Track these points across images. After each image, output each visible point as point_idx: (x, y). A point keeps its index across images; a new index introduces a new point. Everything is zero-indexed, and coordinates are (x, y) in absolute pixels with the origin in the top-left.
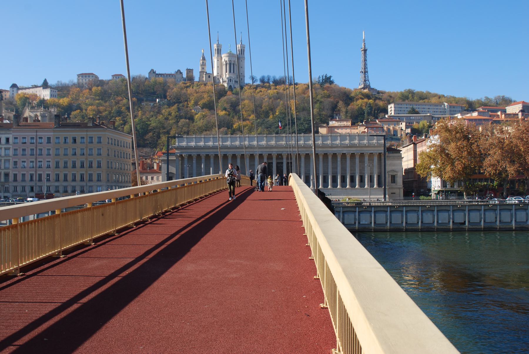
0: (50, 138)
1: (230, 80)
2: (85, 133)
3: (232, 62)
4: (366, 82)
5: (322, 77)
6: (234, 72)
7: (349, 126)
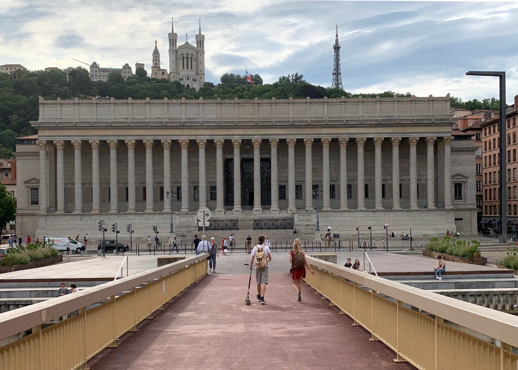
1: (188, 77)
3: (190, 56)
4: (339, 86)
5: (292, 77)
6: (191, 69)
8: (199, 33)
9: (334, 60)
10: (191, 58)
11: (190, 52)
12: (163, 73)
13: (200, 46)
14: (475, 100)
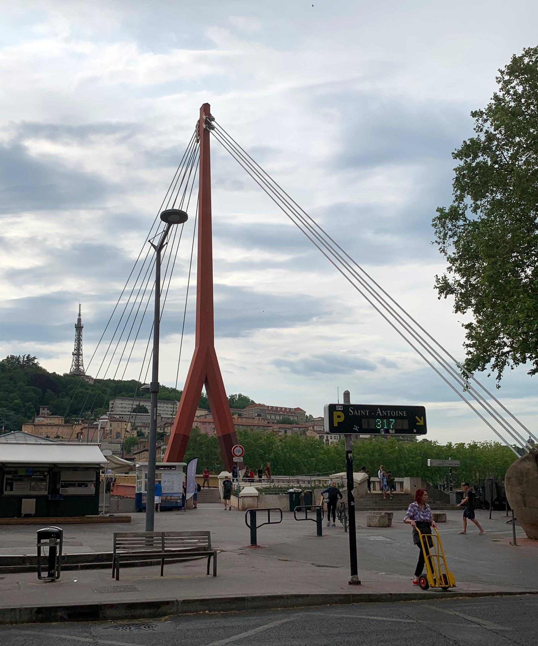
4: (80, 367)
5: (23, 358)
9: (76, 340)
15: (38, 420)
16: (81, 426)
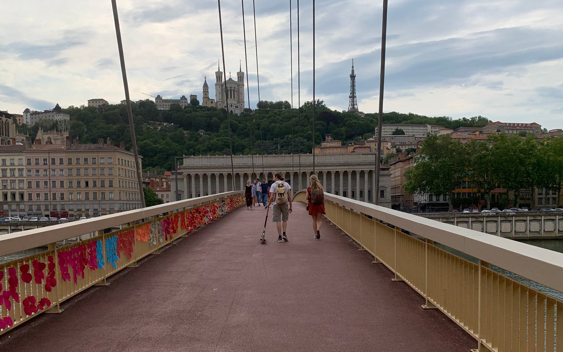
0: (63, 159)
1: (231, 105)
2: (97, 154)
3: (233, 89)
6: (234, 98)
7: (339, 147)
8: (239, 71)
10: (234, 91)
11: (233, 86)
12: (212, 102)
13: (241, 81)
14: (464, 118)
15: (324, 144)
16: (353, 147)
